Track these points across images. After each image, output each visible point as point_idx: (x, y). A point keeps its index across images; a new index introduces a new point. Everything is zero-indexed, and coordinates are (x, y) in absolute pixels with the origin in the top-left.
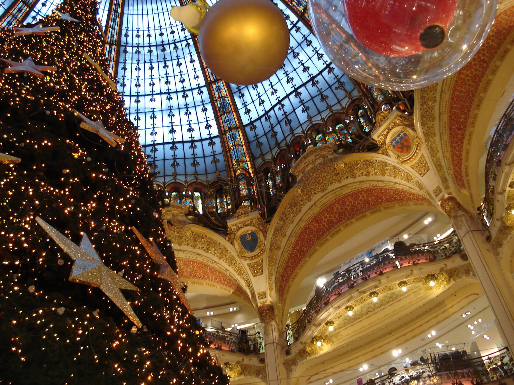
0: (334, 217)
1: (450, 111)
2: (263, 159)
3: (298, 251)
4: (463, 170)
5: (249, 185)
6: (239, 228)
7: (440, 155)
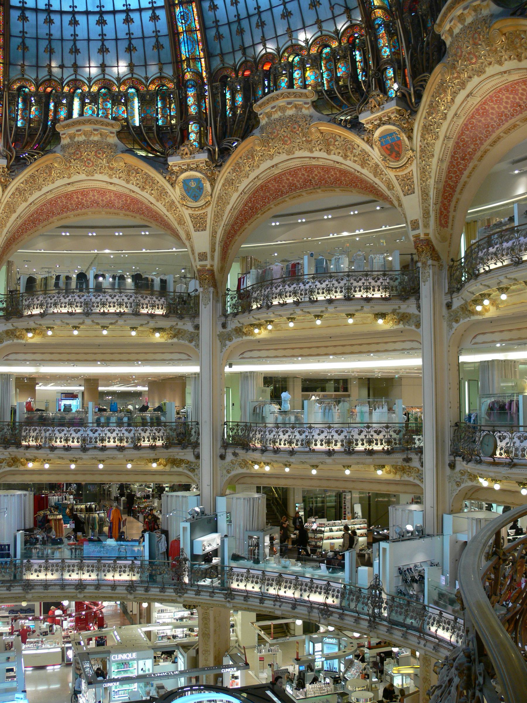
0: (298, 181)
1: (459, 137)
2: (222, 61)
3: (250, 208)
4: (453, 204)
5: (200, 97)
6: (183, 171)
7: (431, 182)
